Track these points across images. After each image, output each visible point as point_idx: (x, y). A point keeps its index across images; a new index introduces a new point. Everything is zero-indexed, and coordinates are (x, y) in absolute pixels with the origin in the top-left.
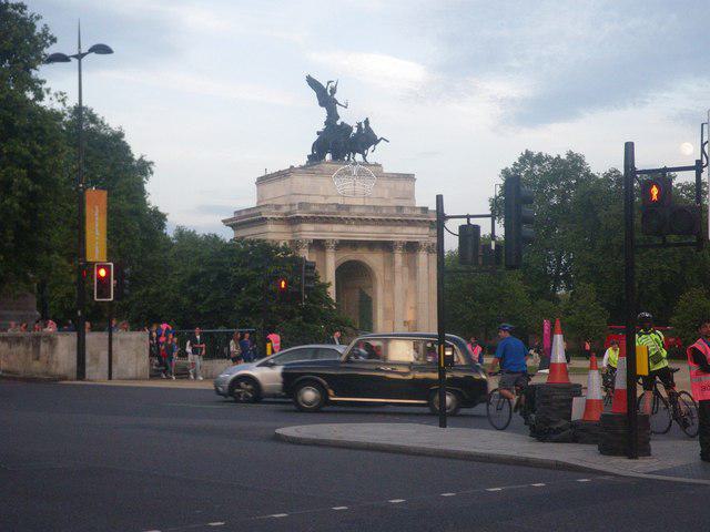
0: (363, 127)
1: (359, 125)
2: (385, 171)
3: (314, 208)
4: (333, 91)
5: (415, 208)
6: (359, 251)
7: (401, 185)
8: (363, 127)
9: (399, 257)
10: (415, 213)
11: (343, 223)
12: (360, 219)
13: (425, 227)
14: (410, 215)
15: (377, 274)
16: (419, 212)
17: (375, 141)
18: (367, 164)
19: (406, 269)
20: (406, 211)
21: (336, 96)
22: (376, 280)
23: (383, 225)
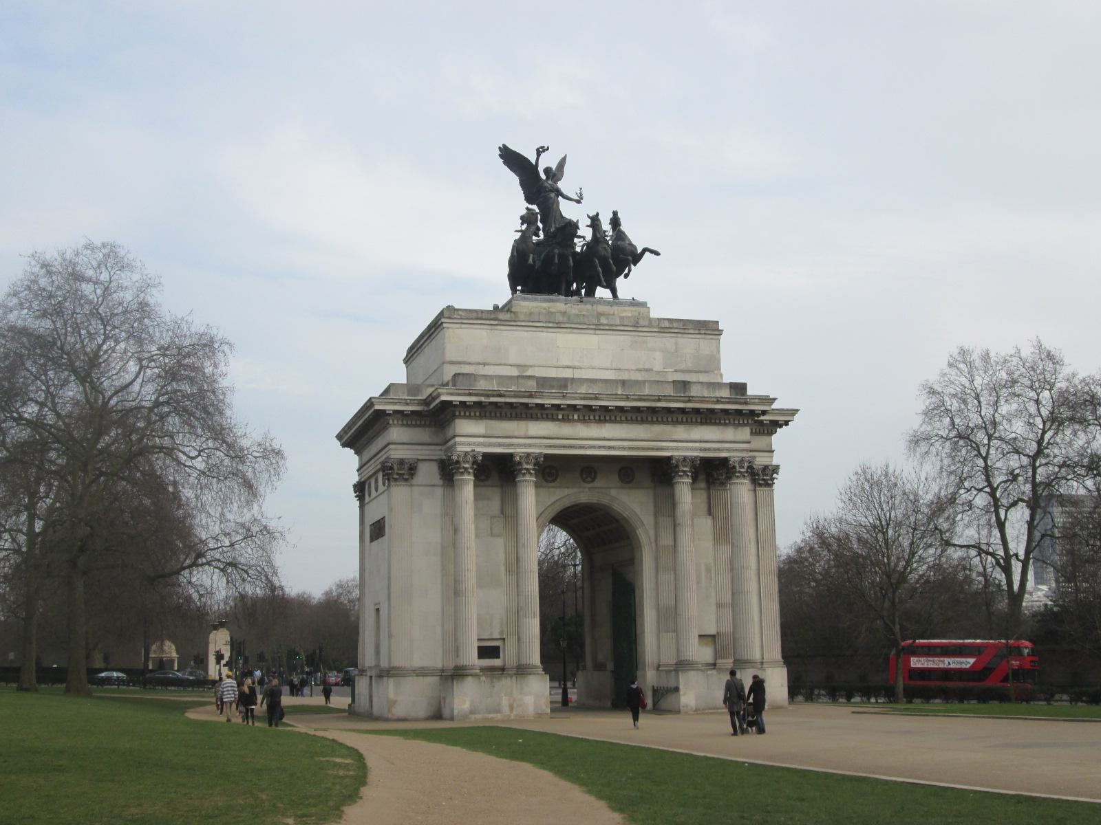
0: (606, 226)
1: (595, 222)
2: (655, 314)
3: (482, 385)
4: (554, 174)
5: (720, 385)
6: (599, 483)
7: (690, 345)
8: (606, 226)
9: (686, 494)
10: (718, 394)
11: (553, 418)
12: (589, 408)
13: (739, 425)
14: (703, 399)
15: (641, 533)
16: (725, 393)
17: (637, 258)
18: (622, 304)
19: (705, 523)
20: (695, 391)
21: (561, 185)
22: (640, 547)
23: (643, 421)
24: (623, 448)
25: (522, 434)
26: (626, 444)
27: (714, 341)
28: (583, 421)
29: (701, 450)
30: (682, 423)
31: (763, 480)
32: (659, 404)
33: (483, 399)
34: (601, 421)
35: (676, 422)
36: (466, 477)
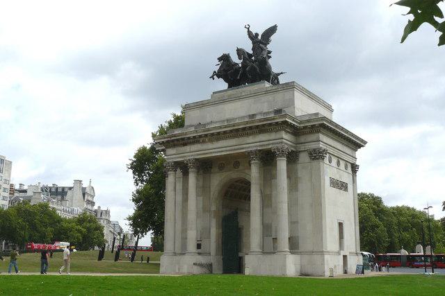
6: (241, 168)
11: (198, 142)
20: (258, 117)
23: (234, 137)
24: (227, 151)
25: (188, 150)
26: (228, 148)
27: (291, 92)
28: (211, 141)
29: (262, 146)
30: (251, 134)
31: (315, 157)
32: (235, 128)
33: (169, 139)
34: (218, 140)
35: (248, 135)
36: (169, 173)
